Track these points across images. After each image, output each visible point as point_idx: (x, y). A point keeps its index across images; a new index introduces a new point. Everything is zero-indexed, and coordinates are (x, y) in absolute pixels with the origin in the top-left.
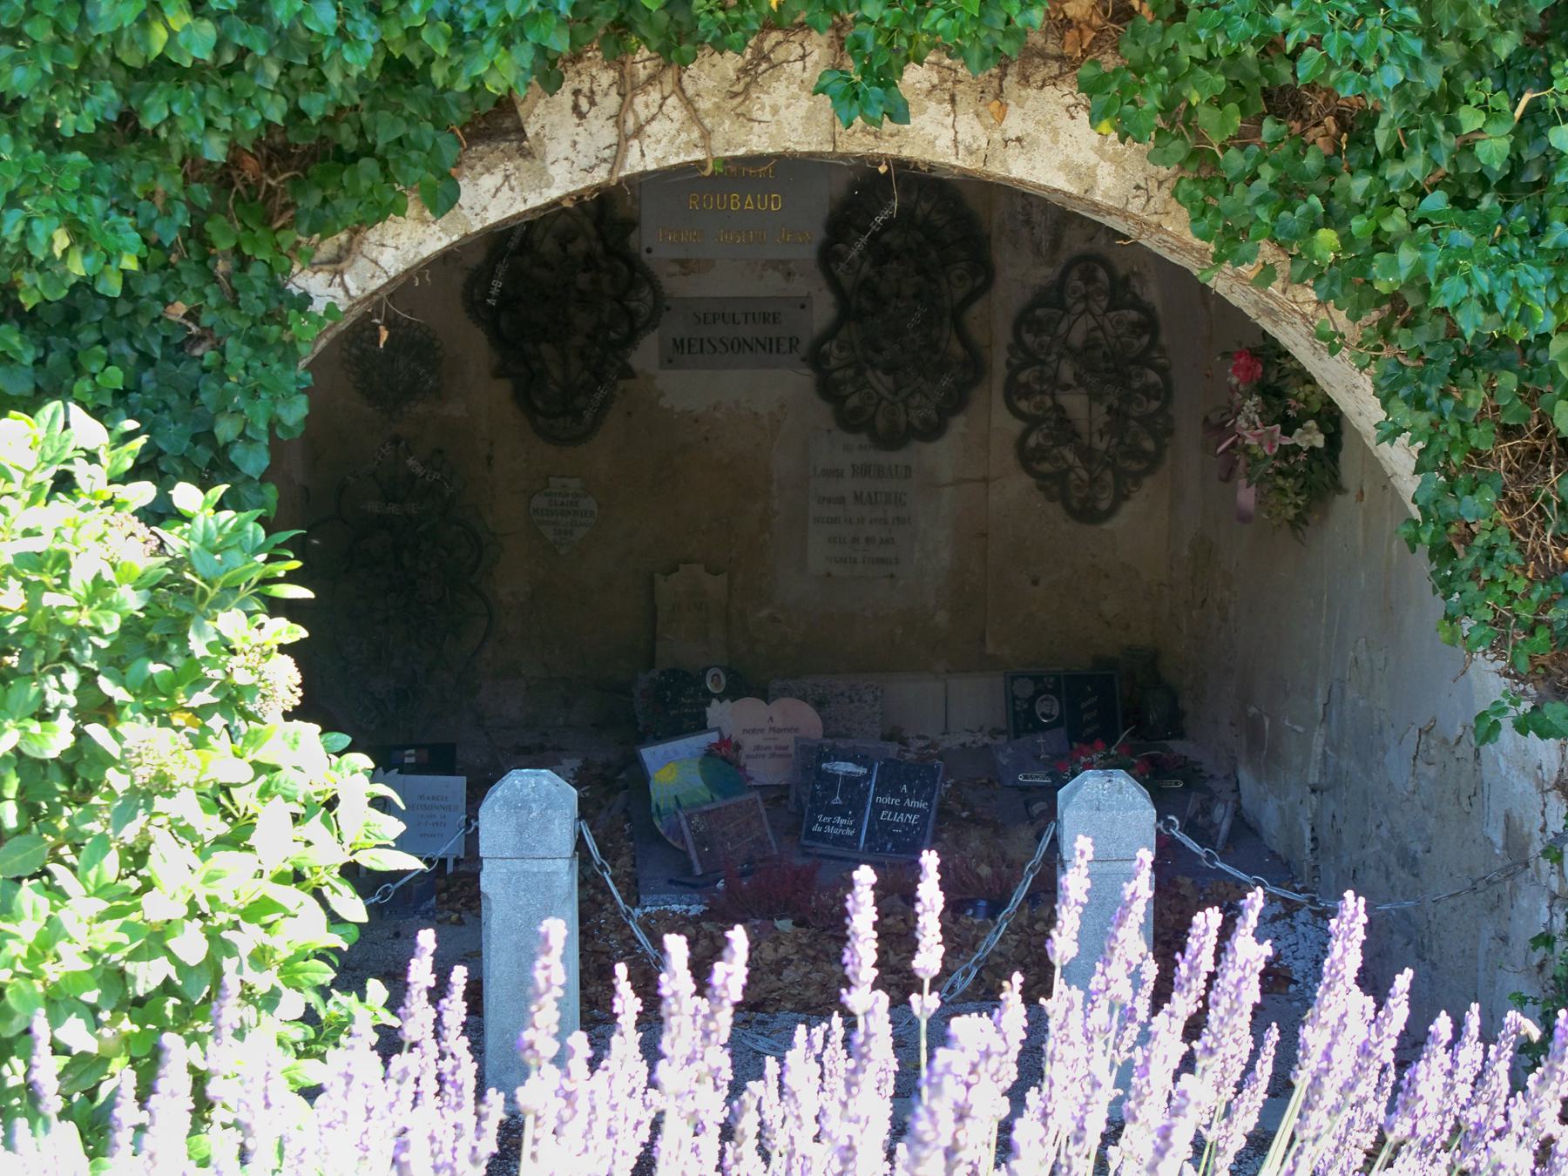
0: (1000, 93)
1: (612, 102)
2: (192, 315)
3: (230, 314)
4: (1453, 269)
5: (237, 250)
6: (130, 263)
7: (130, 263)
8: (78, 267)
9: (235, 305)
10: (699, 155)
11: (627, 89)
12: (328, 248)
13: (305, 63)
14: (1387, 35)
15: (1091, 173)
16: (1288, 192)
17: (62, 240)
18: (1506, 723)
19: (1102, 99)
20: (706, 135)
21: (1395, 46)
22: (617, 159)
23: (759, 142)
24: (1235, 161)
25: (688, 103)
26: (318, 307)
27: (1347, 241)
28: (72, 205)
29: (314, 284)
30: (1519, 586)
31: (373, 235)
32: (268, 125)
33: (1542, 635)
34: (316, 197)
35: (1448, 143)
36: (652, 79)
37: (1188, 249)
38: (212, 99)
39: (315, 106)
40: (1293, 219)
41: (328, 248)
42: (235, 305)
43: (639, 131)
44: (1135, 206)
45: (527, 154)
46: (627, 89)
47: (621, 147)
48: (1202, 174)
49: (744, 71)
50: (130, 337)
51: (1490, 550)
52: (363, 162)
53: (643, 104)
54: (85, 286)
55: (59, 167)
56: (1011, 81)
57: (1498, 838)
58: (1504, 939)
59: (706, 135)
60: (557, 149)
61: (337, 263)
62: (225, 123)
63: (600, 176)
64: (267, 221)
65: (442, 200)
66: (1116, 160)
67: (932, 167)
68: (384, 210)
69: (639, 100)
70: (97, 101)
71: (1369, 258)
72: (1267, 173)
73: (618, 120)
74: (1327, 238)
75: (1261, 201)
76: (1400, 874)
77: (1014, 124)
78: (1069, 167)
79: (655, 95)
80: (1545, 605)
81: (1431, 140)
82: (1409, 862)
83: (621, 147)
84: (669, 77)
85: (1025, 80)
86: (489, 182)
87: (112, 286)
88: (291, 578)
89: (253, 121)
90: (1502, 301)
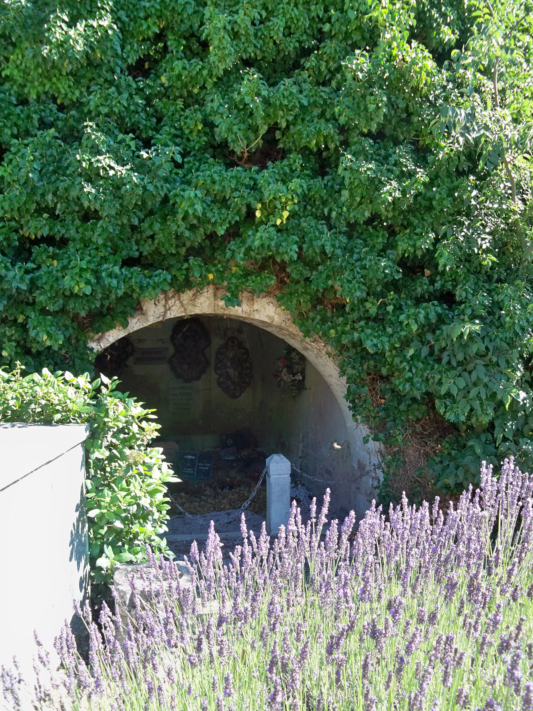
0: (253, 300)
1: (163, 302)
2: (67, 352)
3: (75, 352)
4: (367, 338)
5: (77, 338)
6: (61, 342)
7: (61, 342)
8: (48, 343)
9: (77, 351)
10: (183, 314)
11: (167, 299)
12: (96, 337)
13: (107, 292)
14: (357, 285)
15: (273, 317)
16: (324, 321)
17: (45, 337)
18: (370, 439)
19: (282, 301)
20: (185, 310)
21: (359, 287)
22: (164, 316)
23: (197, 311)
24: (311, 314)
25: (181, 302)
26: (95, 351)
27: (337, 331)
28: (48, 329)
29: (93, 345)
30: (372, 408)
31: (107, 334)
32: (96, 307)
33: (377, 419)
34: (97, 325)
35: (362, 309)
36: (173, 297)
37: (291, 334)
38: (84, 302)
39: (106, 303)
40: (325, 327)
41: (96, 337)
42: (77, 351)
43: (169, 309)
44: (283, 325)
45: (143, 314)
46: (167, 299)
47: (165, 312)
48: (301, 319)
49: (194, 295)
50: (52, 359)
51: (365, 401)
52: (108, 316)
53: (171, 302)
54: (49, 348)
55: (45, 320)
56: (255, 297)
57: (356, 466)
58: (358, 488)
59: (185, 310)
60: (150, 313)
61: (99, 340)
62: (86, 308)
63: (161, 319)
64: (83, 331)
65: (125, 325)
66: (279, 314)
67: (237, 316)
68: (112, 327)
69: (170, 302)
70: (58, 303)
71: (341, 336)
72: (319, 317)
73: (165, 306)
74: (332, 331)
75: (317, 323)
76: (326, 476)
77: (256, 307)
78: (268, 316)
79: (173, 300)
80: (378, 412)
81: (359, 309)
82: (329, 472)
83: (165, 312)
84: (177, 296)
85: (259, 297)
86: (134, 321)
87: (56, 348)
88: (152, 413)
89: (93, 307)
90: (379, 345)
